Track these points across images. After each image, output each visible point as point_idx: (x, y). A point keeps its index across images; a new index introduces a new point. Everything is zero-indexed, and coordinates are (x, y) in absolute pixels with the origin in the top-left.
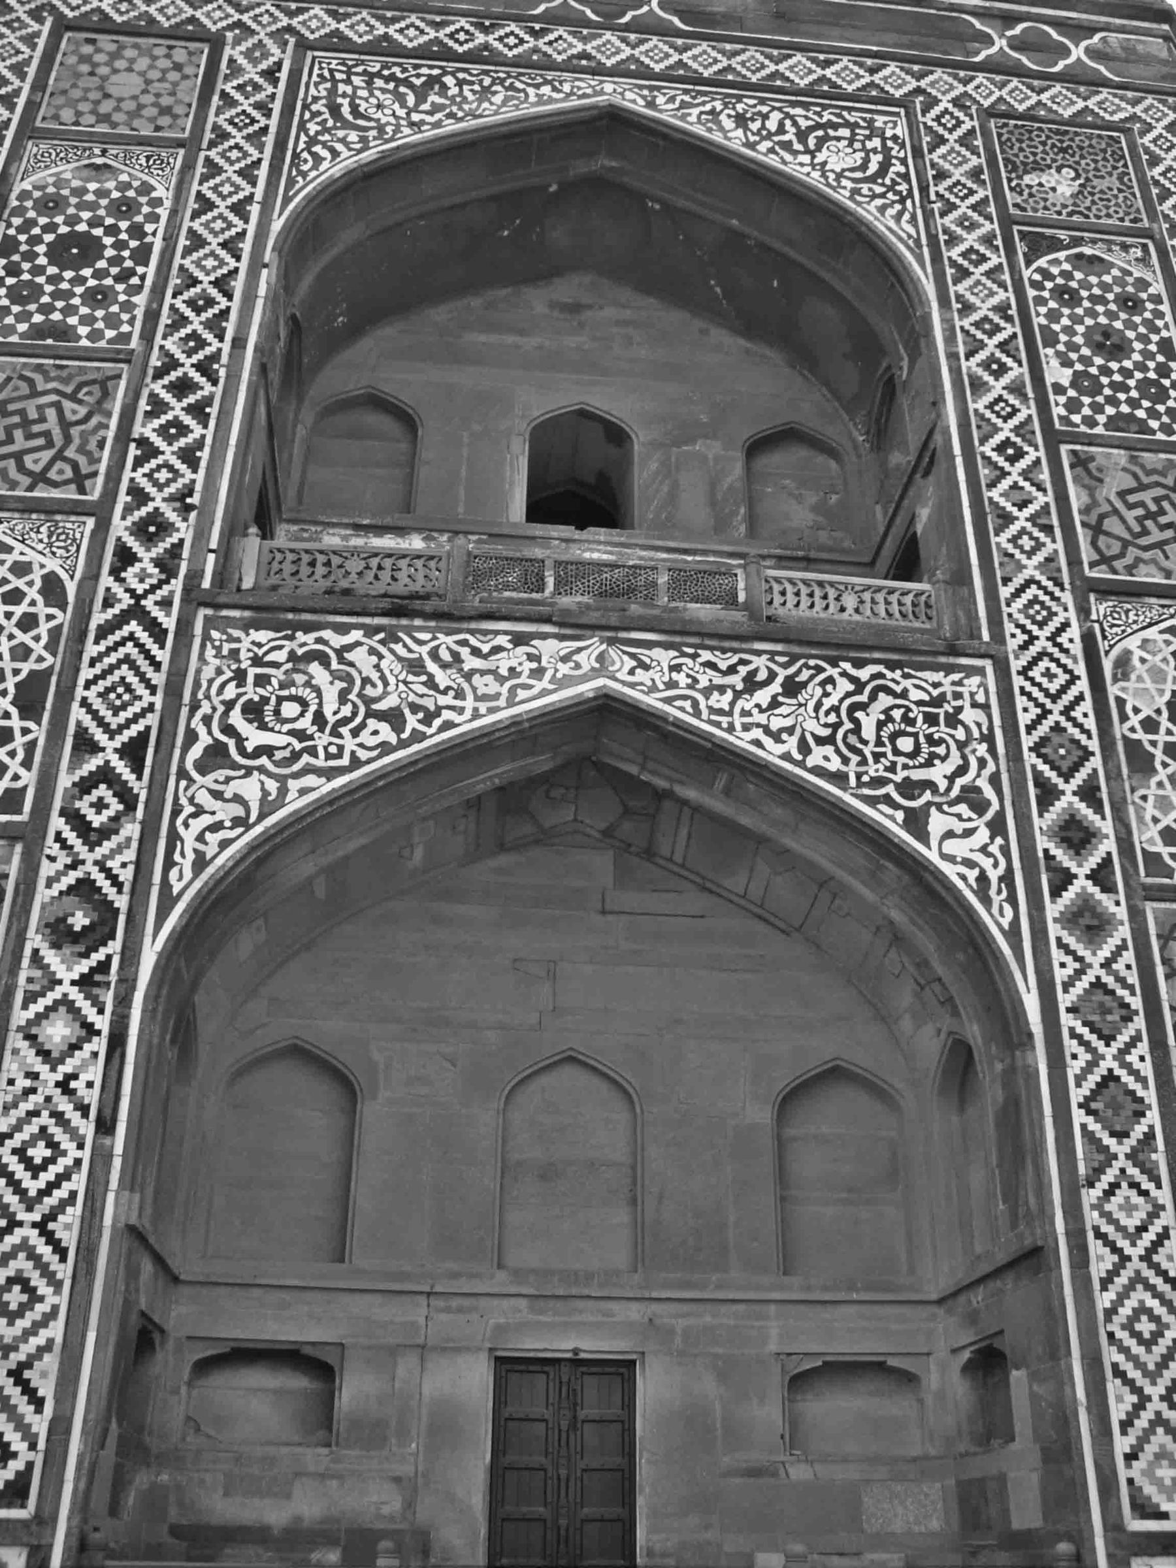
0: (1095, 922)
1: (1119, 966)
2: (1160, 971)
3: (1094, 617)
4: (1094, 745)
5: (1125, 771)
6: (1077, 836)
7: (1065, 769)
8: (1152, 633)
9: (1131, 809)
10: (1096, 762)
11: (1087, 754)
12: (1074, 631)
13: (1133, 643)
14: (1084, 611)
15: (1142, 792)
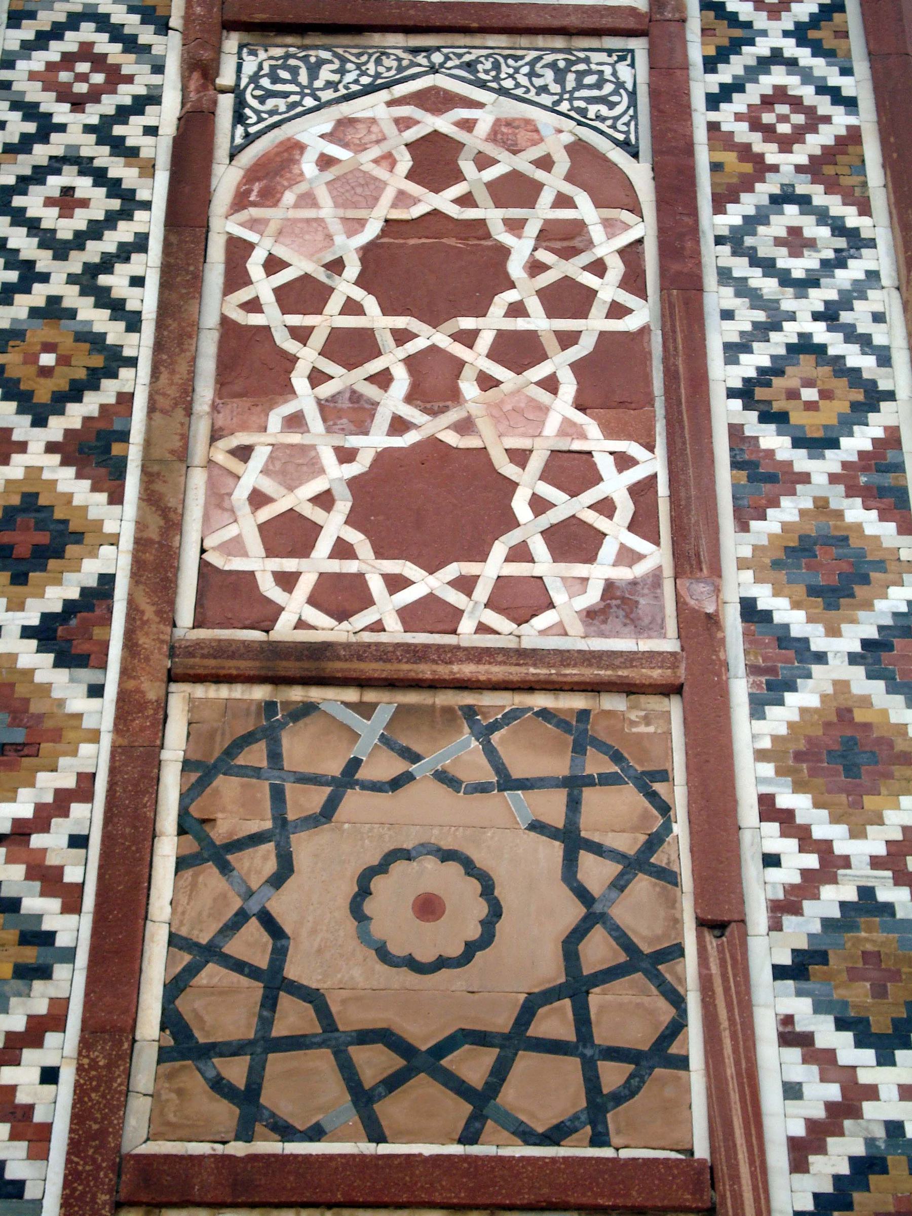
0: (18, 736)
1: (51, 842)
2: (167, 849)
3: (226, 78)
4: (141, 345)
5: (205, 392)
6: (24, 540)
7: (43, 395)
8: (373, 107)
9: (198, 479)
10: (136, 381)
11: (115, 361)
12: (168, 114)
13: (311, 131)
14: (201, 68)
15: (241, 439)
